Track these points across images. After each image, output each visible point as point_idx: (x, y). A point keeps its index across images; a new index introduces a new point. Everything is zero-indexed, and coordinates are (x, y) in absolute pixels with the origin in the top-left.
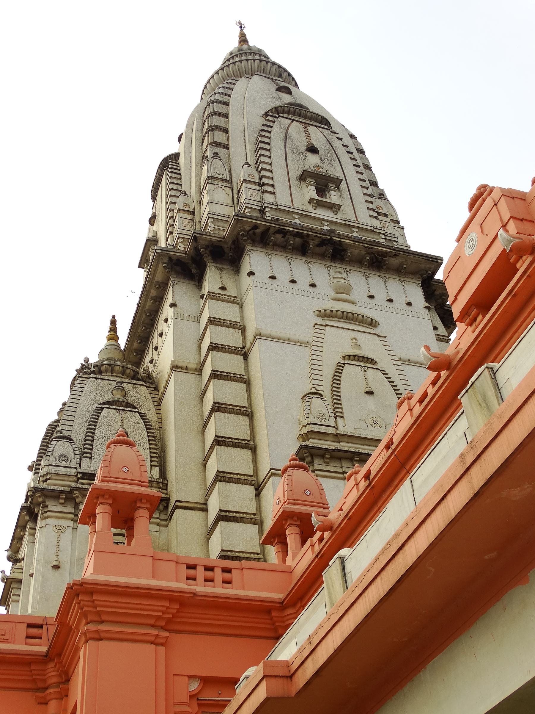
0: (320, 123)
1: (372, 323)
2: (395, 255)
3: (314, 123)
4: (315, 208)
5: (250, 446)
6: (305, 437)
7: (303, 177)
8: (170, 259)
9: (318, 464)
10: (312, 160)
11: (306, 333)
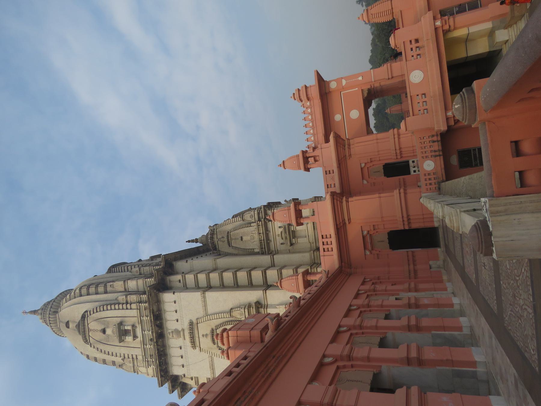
0: (84, 320)
1: (191, 323)
2: (153, 310)
4: (137, 337)
7: (121, 341)
8: (181, 392)
10: (109, 331)
11: (205, 356)
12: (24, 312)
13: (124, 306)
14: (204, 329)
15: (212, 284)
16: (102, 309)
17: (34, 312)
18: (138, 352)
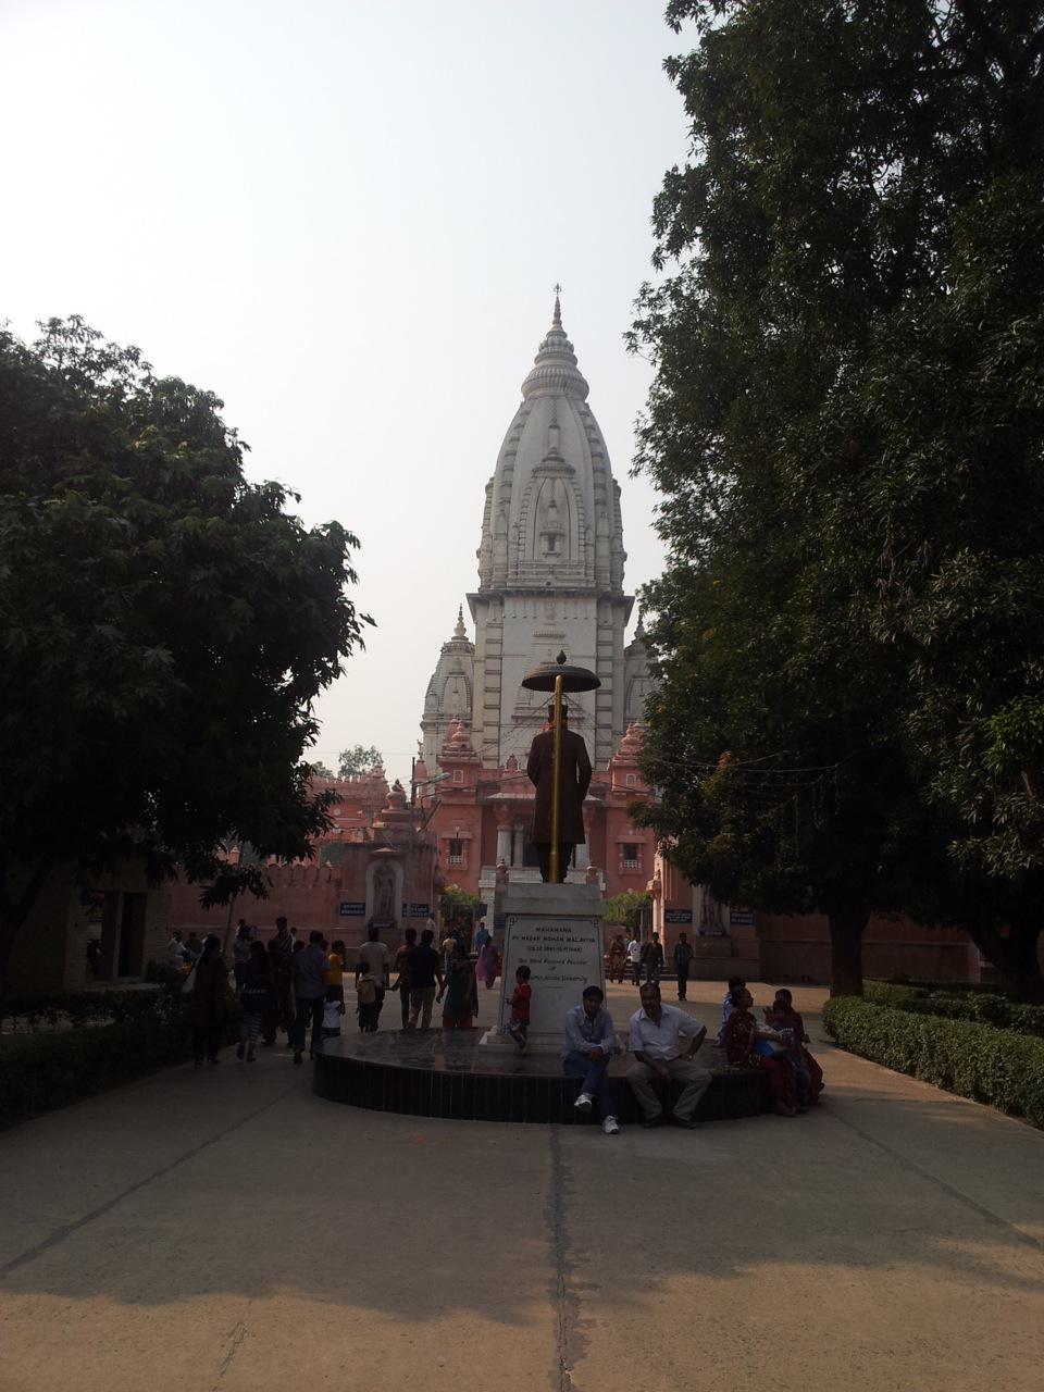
1: (562, 637)
3: (562, 474)
5: (498, 707)
6: (517, 708)
7: (541, 535)
10: (552, 513)
12: (558, 287)
13: (583, 542)
15: (601, 663)
16: (580, 505)
17: (558, 314)
18: (526, 555)
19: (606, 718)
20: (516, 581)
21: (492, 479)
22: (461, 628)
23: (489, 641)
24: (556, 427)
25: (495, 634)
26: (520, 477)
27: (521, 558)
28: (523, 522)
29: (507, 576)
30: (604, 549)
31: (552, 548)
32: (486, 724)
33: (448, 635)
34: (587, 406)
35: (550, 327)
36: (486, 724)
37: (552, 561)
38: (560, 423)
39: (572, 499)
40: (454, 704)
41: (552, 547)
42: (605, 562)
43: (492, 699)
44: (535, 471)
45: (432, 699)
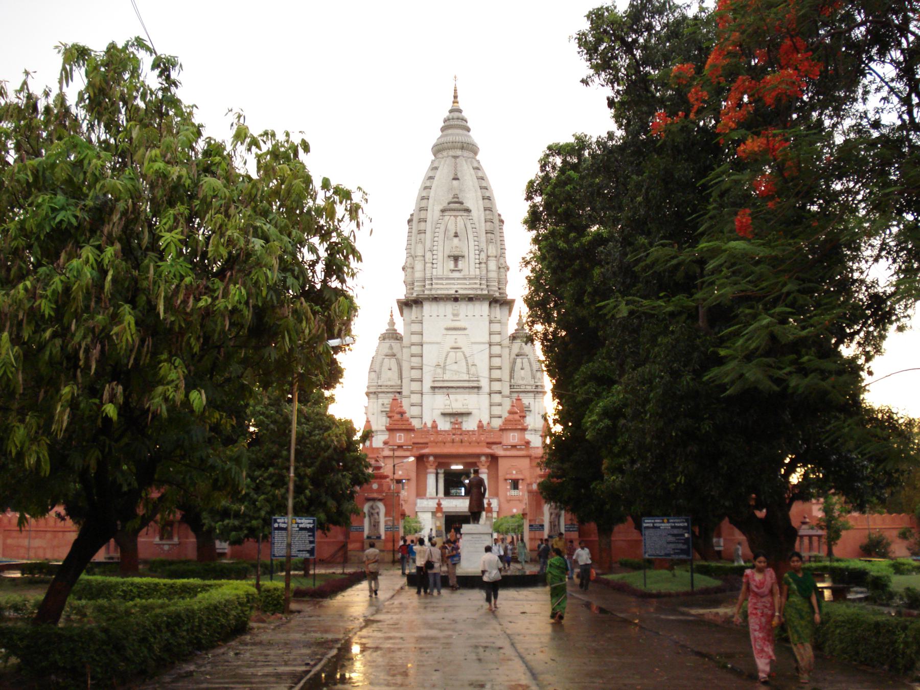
1: (465, 329)
7: (449, 257)
9: (436, 390)
10: (456, 240)
13: (477, 261)
14: (462, 341)
15: (492, 347)
17: (455, 97)
18: (438, 272)
19: (496, 386)
20: (431, 290)
21: (412, 215)
22: (392, 323)
23: (412, 333)
24: (456, 179)
25: (416, 327)
26: (434, 212)
27: (435, 273)
28: (435, 248)
29: (424, 286)
30: (492, 265)
31: (456, 265)
32: (412, 392)
33: (384, 328)
34: (478, 162)
35: (450, 106)
36: (412, 392)
37: (456, 275)
38: (459, 176)
39: (470, 231)
40: (389, 377)
41: (456, 265)
42: (493, 275)
43: (415, 374)
44: (443, 211)
45: (373, 375)
